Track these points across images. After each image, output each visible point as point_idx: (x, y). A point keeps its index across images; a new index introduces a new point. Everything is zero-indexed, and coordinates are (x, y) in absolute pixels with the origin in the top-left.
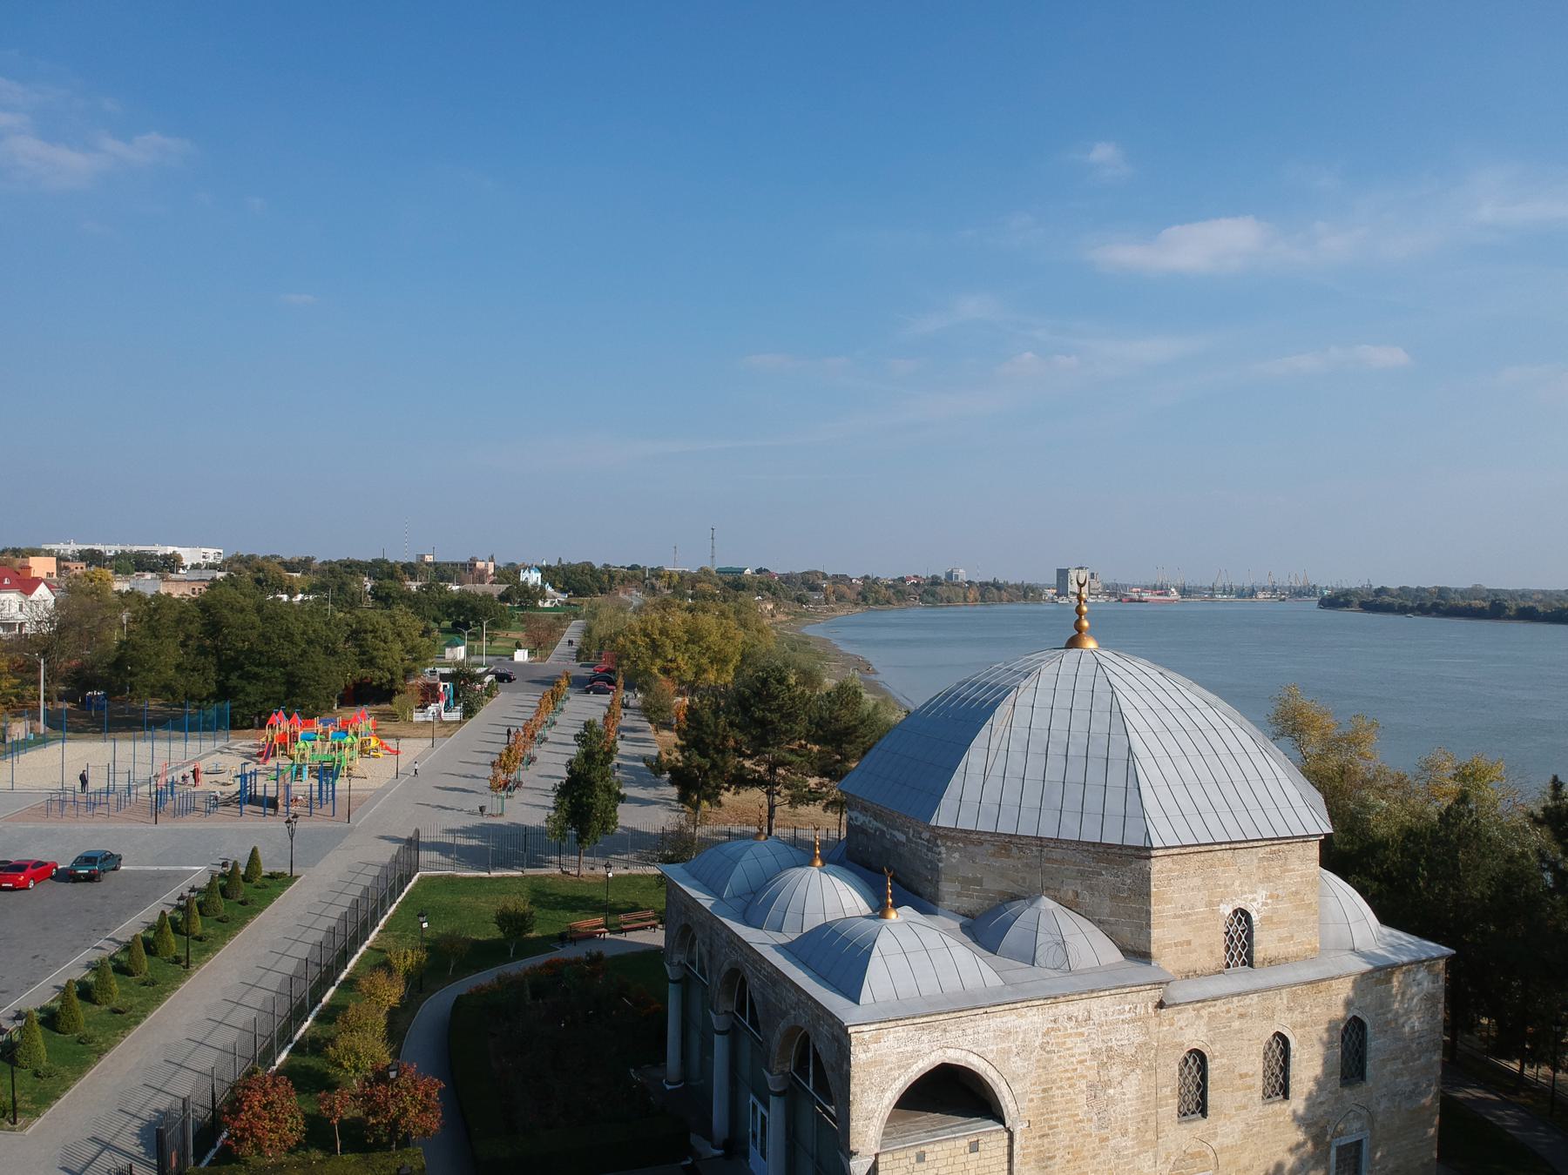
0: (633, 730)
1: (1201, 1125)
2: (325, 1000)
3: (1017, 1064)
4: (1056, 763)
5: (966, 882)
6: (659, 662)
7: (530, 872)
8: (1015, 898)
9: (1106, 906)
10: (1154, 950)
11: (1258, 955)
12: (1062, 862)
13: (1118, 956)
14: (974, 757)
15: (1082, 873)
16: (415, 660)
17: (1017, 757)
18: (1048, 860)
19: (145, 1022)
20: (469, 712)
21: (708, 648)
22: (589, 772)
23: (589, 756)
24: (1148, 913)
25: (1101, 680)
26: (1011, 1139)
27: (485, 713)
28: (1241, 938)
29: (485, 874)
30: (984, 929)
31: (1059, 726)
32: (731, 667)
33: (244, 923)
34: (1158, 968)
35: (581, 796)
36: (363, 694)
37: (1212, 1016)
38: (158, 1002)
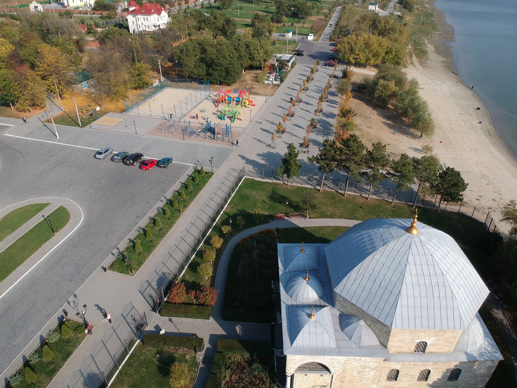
0: (333, 94)
1: (394, 382)
2: (208, 234)
4: (376, 287)
5: (342, 305)
6: (352, 56)
7: (275, 181)
8: (354, 316)
9: (378, 331)
10: (388, 346)
11: (427, 351)
13: (379, 343)
14: (353, 274)
16: (267, 56)
17: (366, 278)
19: (167, 235)
20: (282, 81)
21: (372, 50)
22: (290, 160)
23: (290, 154)
24: (388, 339)
25: (405, 257)
27: (288, 80)
28: (422, 347)
29: (261, 180)
30: (345, 320)
31: (382, 273)
32: (381, 57)
33: (197, 195)
34: (388, 351)
35: (288, 165)
36: (251, 68)
38: (171, 227)
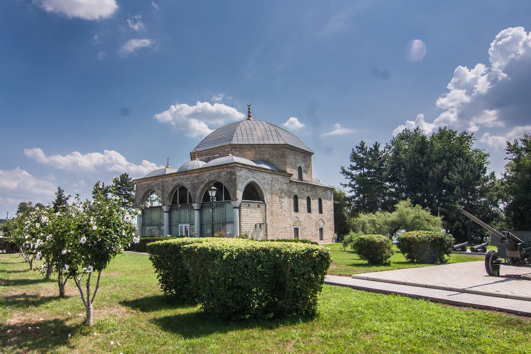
3: (266, 187)
12: (264, 151)
15: (269, 153)
18: (261, 151)
26: (266, 206)
37: (299, 188)
